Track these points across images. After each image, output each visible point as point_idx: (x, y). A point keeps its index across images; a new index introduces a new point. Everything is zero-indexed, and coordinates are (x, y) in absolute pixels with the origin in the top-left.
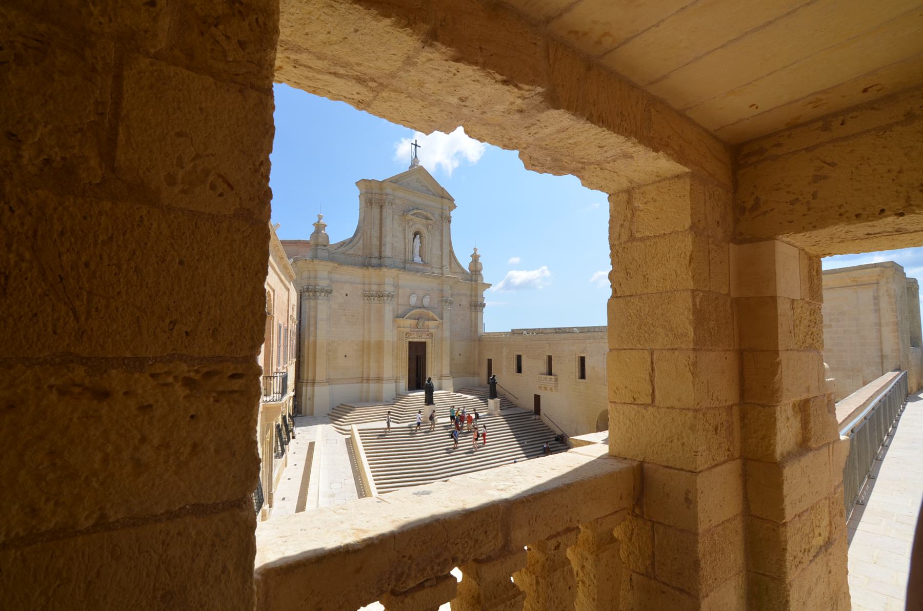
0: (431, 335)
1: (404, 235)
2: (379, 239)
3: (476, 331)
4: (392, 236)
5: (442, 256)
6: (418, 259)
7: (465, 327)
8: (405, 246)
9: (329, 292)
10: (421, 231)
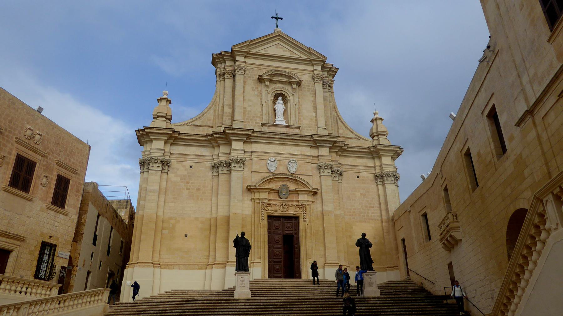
0: (302, 207)
1: (261, 99)
2: (231, 107)
4: (244, 100)
5: (316, 117)
8: (262, 110)
9: (166, 164)
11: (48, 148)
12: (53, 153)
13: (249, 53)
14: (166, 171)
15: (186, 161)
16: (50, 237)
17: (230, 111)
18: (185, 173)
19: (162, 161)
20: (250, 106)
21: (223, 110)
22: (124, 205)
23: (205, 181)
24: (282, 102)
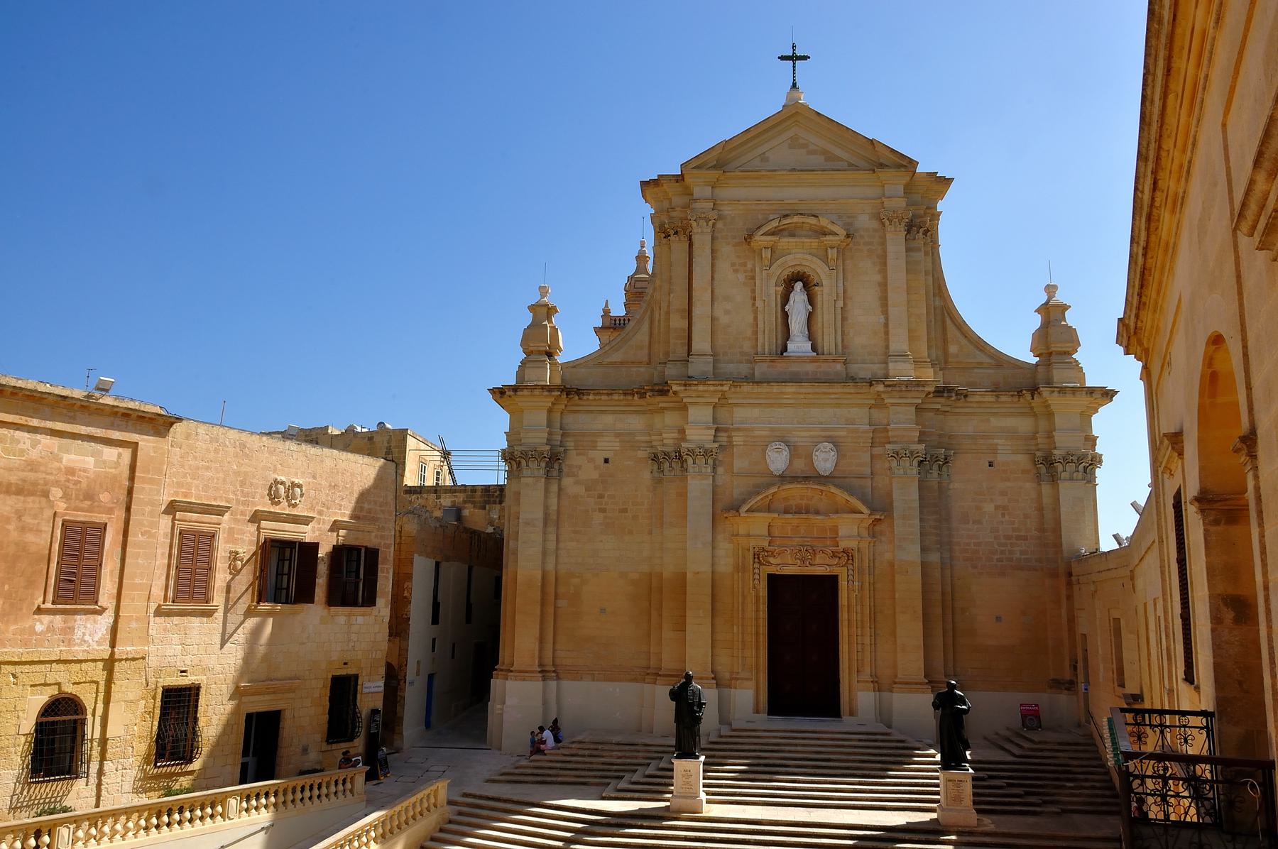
0: (848, 554)
1: (753, 291)
3: (1058, 545)
5: (886, 325)
7: (1014, 530)
8: (756, 319)
10: (806, 270)
11: (317, 503)
12: (328, 508)
14: (555, 473)
15: (594, 447)
16: (345, 664)
17: (685, 324)
18: (595, 475)
19: (545, 457)
20: (727, 312)
21: (668, 319)
22: (497, 497)
23: (636, 491)
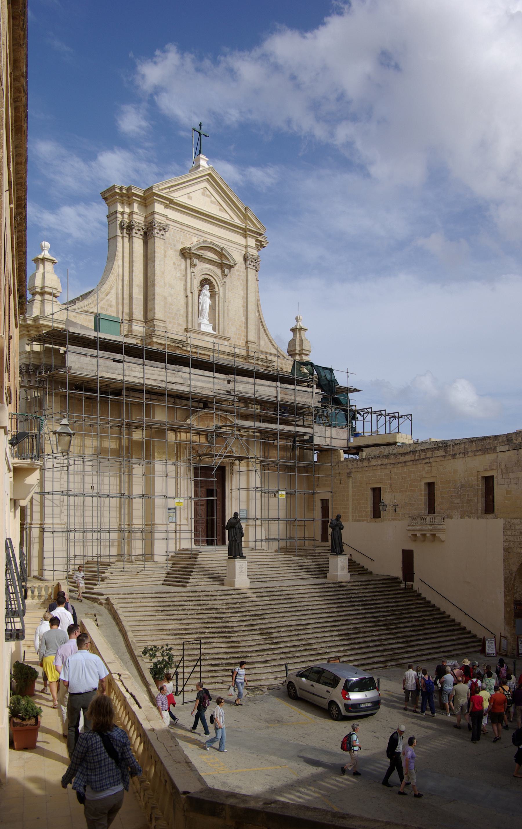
6: (206, 327)
13: (171, 201)
24: (208, 293)
